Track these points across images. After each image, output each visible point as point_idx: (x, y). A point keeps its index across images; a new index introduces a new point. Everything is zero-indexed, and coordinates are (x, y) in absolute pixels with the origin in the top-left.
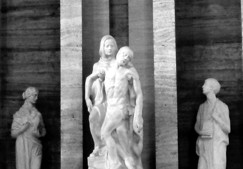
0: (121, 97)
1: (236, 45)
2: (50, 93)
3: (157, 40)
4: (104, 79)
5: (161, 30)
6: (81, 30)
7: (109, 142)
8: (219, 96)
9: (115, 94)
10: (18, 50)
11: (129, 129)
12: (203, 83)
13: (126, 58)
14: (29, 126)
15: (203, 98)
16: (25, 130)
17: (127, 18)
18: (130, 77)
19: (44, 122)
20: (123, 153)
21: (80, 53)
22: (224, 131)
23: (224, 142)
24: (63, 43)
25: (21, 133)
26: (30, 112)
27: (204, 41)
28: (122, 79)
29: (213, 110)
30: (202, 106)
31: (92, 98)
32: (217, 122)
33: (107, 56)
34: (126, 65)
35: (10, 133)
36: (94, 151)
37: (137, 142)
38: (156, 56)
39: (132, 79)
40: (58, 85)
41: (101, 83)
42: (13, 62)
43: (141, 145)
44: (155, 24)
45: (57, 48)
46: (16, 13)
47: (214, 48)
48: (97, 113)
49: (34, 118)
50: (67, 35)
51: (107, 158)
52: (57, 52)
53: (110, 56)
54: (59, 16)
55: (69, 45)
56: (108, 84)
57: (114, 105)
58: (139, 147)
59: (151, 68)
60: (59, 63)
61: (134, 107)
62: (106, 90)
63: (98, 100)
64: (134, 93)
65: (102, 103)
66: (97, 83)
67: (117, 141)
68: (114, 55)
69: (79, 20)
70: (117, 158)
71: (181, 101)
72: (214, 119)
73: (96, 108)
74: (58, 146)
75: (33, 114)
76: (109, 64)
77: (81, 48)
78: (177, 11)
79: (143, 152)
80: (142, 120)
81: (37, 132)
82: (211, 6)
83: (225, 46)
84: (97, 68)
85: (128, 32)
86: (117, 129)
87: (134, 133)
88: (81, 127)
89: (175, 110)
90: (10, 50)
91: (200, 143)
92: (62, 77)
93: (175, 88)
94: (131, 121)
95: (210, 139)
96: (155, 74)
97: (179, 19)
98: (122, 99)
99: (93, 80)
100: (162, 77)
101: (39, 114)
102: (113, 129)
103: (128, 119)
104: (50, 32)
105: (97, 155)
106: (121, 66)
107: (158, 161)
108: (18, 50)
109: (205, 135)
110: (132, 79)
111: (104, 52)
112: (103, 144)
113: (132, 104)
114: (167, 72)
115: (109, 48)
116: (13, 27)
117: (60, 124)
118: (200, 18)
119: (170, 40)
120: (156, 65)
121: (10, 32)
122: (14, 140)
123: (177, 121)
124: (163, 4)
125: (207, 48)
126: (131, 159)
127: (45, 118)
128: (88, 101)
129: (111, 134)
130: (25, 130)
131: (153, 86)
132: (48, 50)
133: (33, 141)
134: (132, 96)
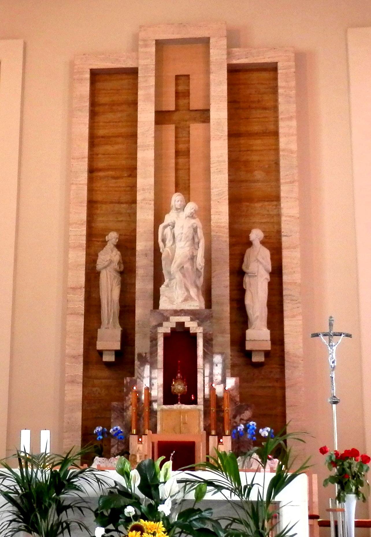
0: (188, 241)
1: (275, 203)
2: (127, 237)
3: (213, 197)
4: (174, 227)
5: (217, 190)
6: (153, 188)
7: (178, 276)
8: (263, 243)
9: (183, 239)
10: (102, 202)
11: (194, 267)
12: (249, 232)
13: (192, 211)
14: (111, 262)
15: (250, 244)
16: (108, 265)
17: (189, 180)
18: (195, 225)
19: (122, 259)
20: (189, 285)
21: (152, 206)
22: (266, 270)
23: (266, 279)
24: (139, 198)
25: (105, 267)
26: (112, 251)
27: (251, 200)
28: (189, 227)
29: (258, 254)
30: (248, 251)
31: (164, 241)
32: (261, 263)
33: (177, 209)
34: (192, 216)
35: (95, 267)
36: (165, 283)
37: (199, 277)
38: (213, 211)
39: (196, 228)
40: (135, 230)
41: (171, 229)
42: (98, 212)
43: (202, 279)
44: (212, 185)
45: (134, 202)
46: (101, 174)
47: (258, 205)
48: (169, 254)
49: (115, 255)
50: (142, 192)
51: (176, 288)
52: (133, 205)
53: (179, 209)
54: (135, 176)
55: (144, 199)
56: (177, 230)
57: (182, 248)
58: (201, 281)
59: (210, 220)
60: (135, 214)
61: (198, 249)
62: (176, 235)
63: (169, 243)
64: (198, 238)
65: (172, 246)
66: (168, 230)
67: (184, 276)
68: (183, 208)
69: (151, 181)
70: (184, 289)
71: (232, 245)
72: (258, 261)
73: (167, 249)
75: (114, 253)
76: (178, 216)
77: (153, 202)
78: (229, 175)
79: (203, 286)
80: (204, 260)
81: (117, 267)
82: (256, 173)
83: (266, 203)
84: (169, 218)
85: (189, 191)
86: (184, 267)
87: (197, 269)
88: (153, 264)
89: (227, 252)
90: (96, 202)
91: (246, 279)
92: (137, 224)
93: (228, 235)
94: (195, 260)
95: (256, 276)
96: (212, 224)
97: (231, 181)
98: (188, 244)
99: (165, 227)
100: (218, 227)
101: (119, 253)
102: (182, 266)
103: (193, 258)
104: (128, 189)
105: (167, 286)
106: (189, 217)
107: (214, 292)
108: (102, 202)
109: (251, 273)
110: (196, 228)
111: (175, 205)
112: (172, 277)
113: (196, 246)
114: (221, 223)
115: (179, 202)
116: (99, 185)
117: (135, 261)
118: (246, 181)
119: (224, 198)
120: (212, 217)
121: (96, 188)
122: (98, 273)
123: (228, 261)
124: (218, 170)
125: (252, 205)
126: (195, 290)
127: (123, 255)
128: (161, 244)
129: (180, 270)
130: (108, 265)
131: (210, 233)
132: (126, 203)
133: (115, 274)
134: (196, 240)
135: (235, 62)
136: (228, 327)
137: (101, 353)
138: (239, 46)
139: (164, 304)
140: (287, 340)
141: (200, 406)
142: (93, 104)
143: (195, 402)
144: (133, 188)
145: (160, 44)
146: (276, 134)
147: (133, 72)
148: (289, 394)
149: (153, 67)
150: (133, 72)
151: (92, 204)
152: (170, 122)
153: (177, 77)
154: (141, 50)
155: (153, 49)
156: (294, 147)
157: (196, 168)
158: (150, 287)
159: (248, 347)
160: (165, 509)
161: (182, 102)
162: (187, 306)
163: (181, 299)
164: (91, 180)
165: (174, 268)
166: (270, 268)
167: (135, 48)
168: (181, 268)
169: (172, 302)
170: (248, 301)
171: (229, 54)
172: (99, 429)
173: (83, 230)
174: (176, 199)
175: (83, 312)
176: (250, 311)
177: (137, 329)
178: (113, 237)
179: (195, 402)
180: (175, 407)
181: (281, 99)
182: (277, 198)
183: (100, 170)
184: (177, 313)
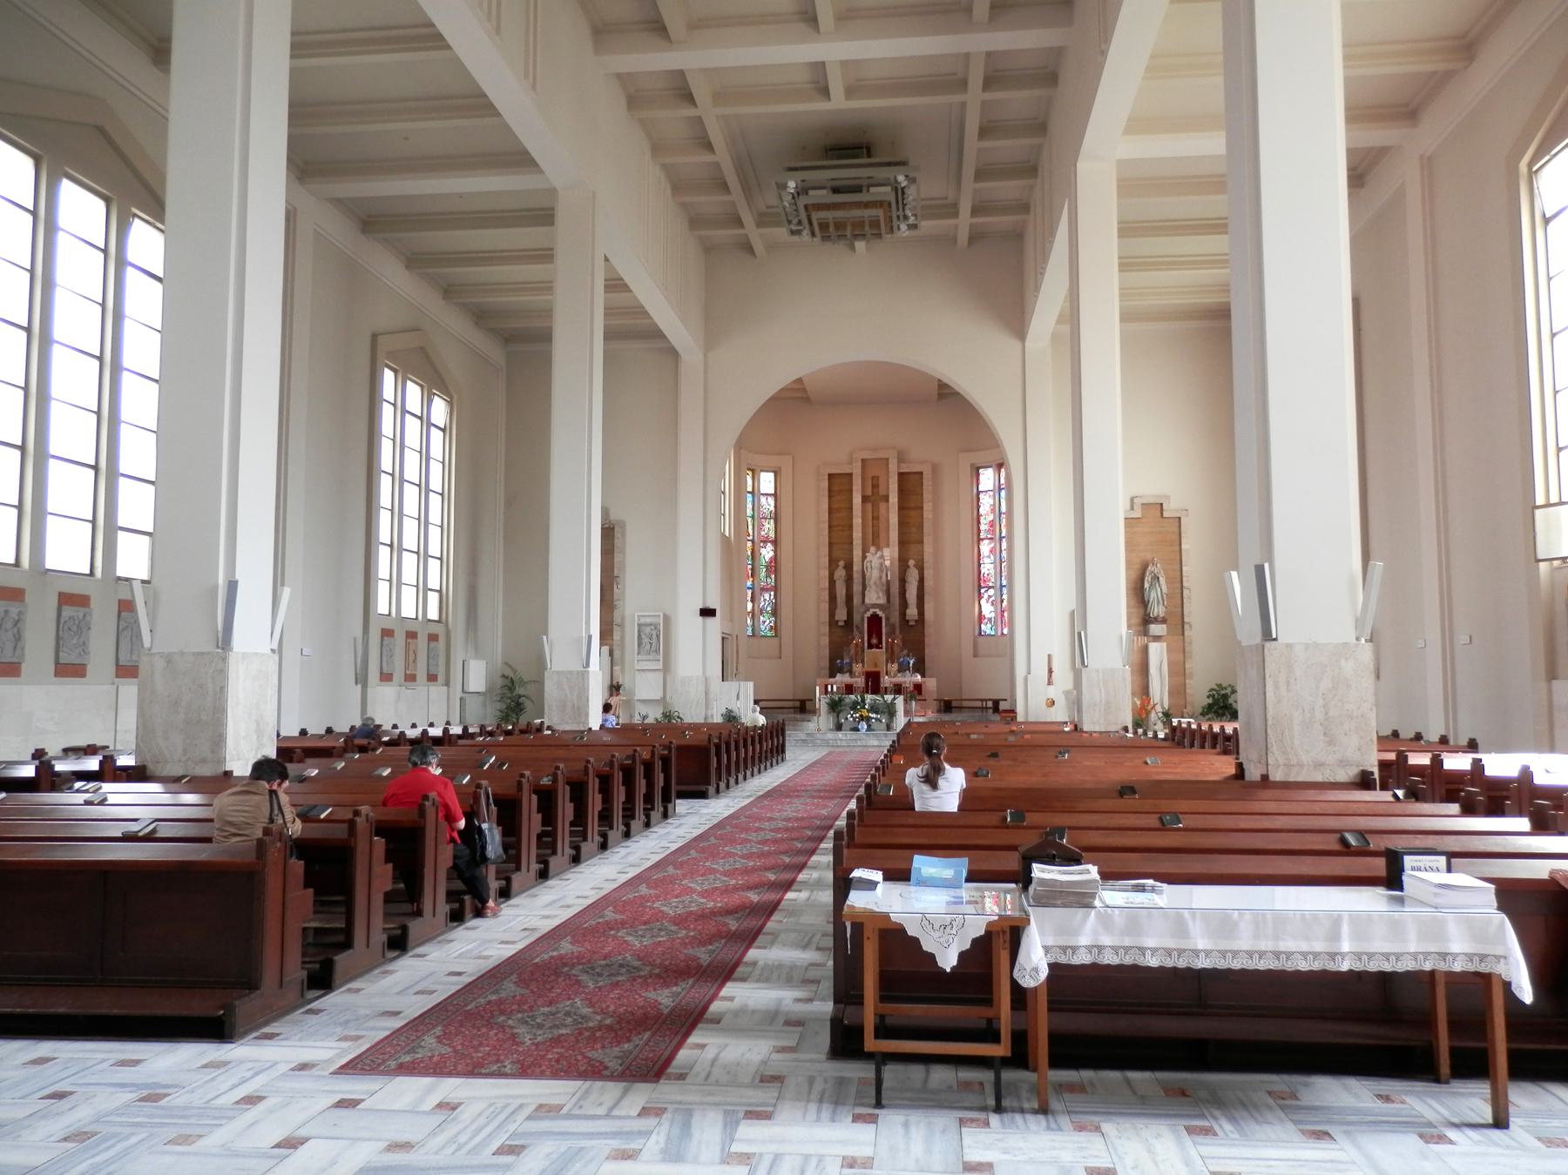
7: (874, 587)
14: (841, 576)
15: (909, 567)
58: (884, 588)
63: (869, 570)
68: (876, 553)
69: (860, 535)
74: (852, 583)
103: (881, 578)
122: (835, 582)
135: (901, 471)
136: (898, 608)
138: (903, 462)
139: (867, 601)
140: (926, 613)
141: (884, 650)
142: (830, 491)
143: (882, 648)
144: (851, 537)
145: (863, 460)
146: (922, 508)
147: (851, 475)
148: (926, 639)
150: (851, 475)
151: (831, 544)
152: (869, 502)
153: (873, 478)
154: (854, 464)
155: (860, 464)
156: (931, 516)
157: (882, 526)
158: (860, 588)
159: (907, 618)
160: (867, 707)
161: (875, 490)
162: (878, 602)
163: (875, 598)
164: (830, 532)
165: (872, 582)
166: (918, 579)
167: (850, 463)
168: (875, 583)
170: (907, 596)
171: (899, 467)
172: (839, 661)
174: (872, 549)
176: (909, 601)
177: (855, 610)
178: (842, 563)
179: (882, 648)
180: (873, 650)
181: (924, 492)
182: (923, 542)
183: (836, 526)
184: (874, 606)
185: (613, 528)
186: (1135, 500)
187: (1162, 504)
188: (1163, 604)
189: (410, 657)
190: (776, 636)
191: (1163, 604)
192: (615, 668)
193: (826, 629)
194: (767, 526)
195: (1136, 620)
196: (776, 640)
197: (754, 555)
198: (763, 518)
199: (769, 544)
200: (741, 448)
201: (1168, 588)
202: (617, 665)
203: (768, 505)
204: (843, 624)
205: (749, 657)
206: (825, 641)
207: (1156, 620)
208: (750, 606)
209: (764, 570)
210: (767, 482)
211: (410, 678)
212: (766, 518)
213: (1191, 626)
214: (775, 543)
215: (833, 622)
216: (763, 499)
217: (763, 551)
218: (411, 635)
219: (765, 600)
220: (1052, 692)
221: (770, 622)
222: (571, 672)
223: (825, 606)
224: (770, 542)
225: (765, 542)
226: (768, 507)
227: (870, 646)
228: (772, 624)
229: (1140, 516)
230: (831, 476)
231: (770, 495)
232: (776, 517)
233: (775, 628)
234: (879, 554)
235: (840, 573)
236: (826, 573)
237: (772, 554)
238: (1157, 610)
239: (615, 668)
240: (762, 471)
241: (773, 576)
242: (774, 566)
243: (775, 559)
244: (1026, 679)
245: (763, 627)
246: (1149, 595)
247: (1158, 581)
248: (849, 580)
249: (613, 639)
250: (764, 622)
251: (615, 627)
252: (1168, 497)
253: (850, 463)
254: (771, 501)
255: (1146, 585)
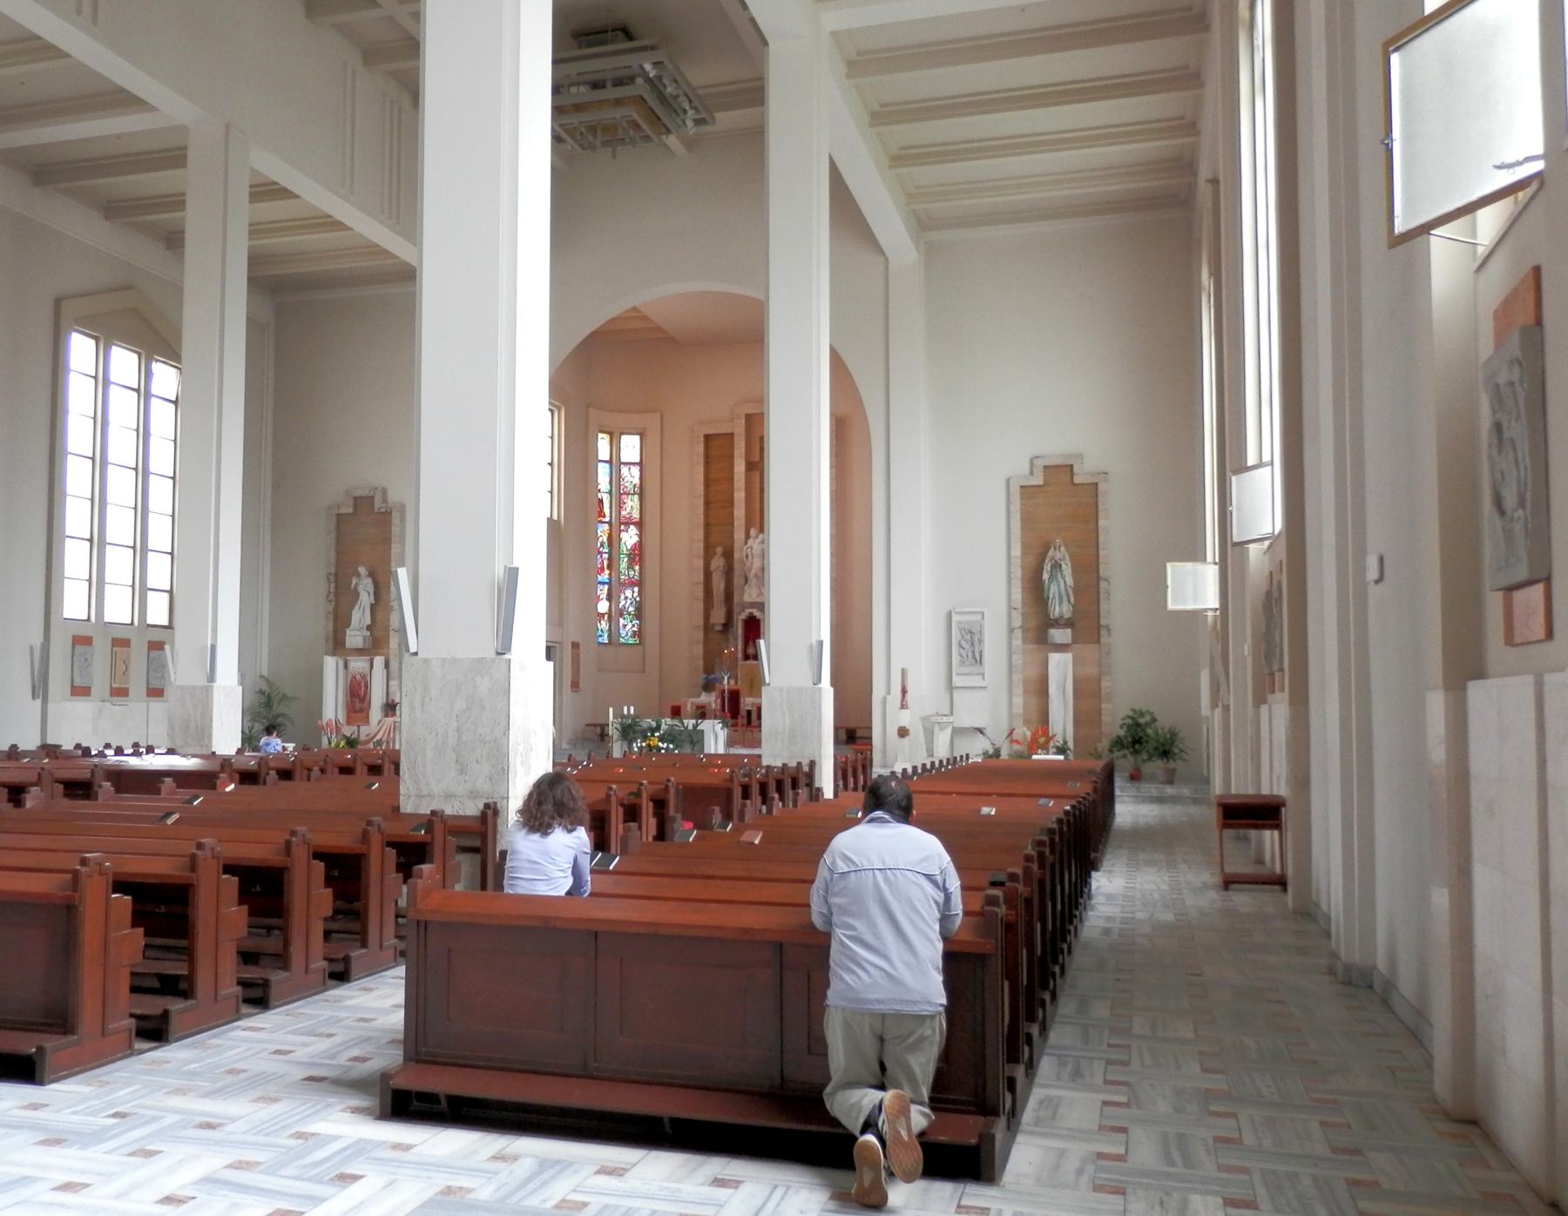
14: (718, 567)
56: (754, 551)
63: (750, 558)
66: (749, 550)
68: (757, 537)
69: (743, 512)
137: (714, 624)
142: (707, 457)
149: (744, 433)
151: (707, 526)
169: (750, 595)
173: (702, 545)
175: (702, 598)
178: (719, 550)
180: (748, 662)
185: (391, 512)
186: (1035, 462)
187: (1072, 466)
188: (1069, 601)
189: (119, 667)
190: (640, 644)
191: (1069, 601)
192: (394, 683)
193: (701, 635)
194: (630, 503)
195: (1033, 624)
196: (640, 648)
197: (613, 541)
198: (625, 493)
199: (632, 527)
200: (588, 407)
201: (1075, 578)
202: (393, 679)
203: (631, 476)
204: (720, 628)
205: (600, 670)
206: (699, 650)
207: (1057, 623)
208: (603, 607)
209: (626, 559)
210: (631, 447)
211: (120, 692)
212: (629, 494)
213: (1109, 630)
214: (640, 525)
215: (708, 628)
216: (624, 470)
217: (623, 535)
218: (121, 643)
219: (626, 598)
220: (905, 719)
221: (633, 626)
222: (194, 687)
223: (699, 606)
224: (633, 524)
225: (627, 524)
226: (631, 479)
227: (747, 657)
228: (635, 629)
229: (1041, 483)
230: (707, 438)
231: (634, 464)
232: (641, 492)
233: (639, 634)
234: (761, 536)
235: (718, 563)
236: (700, 563)
237: (636, 539)
238: (1060, 608)
239: (391, 683)
240: (622, 434)
241: (637, 568)
242: (637, 554)
243: (639, 546)
244: (884, 700)
245: (623, 633)
246: (1049, 590)
247: (1061, 571)
248: (729, 572)
249: (389, 648)
250: (626, 625)
251: (392, 633)
252: (1080, 456)
253: (732, 420)
254: (636, 471)
255: (1046, 576)
